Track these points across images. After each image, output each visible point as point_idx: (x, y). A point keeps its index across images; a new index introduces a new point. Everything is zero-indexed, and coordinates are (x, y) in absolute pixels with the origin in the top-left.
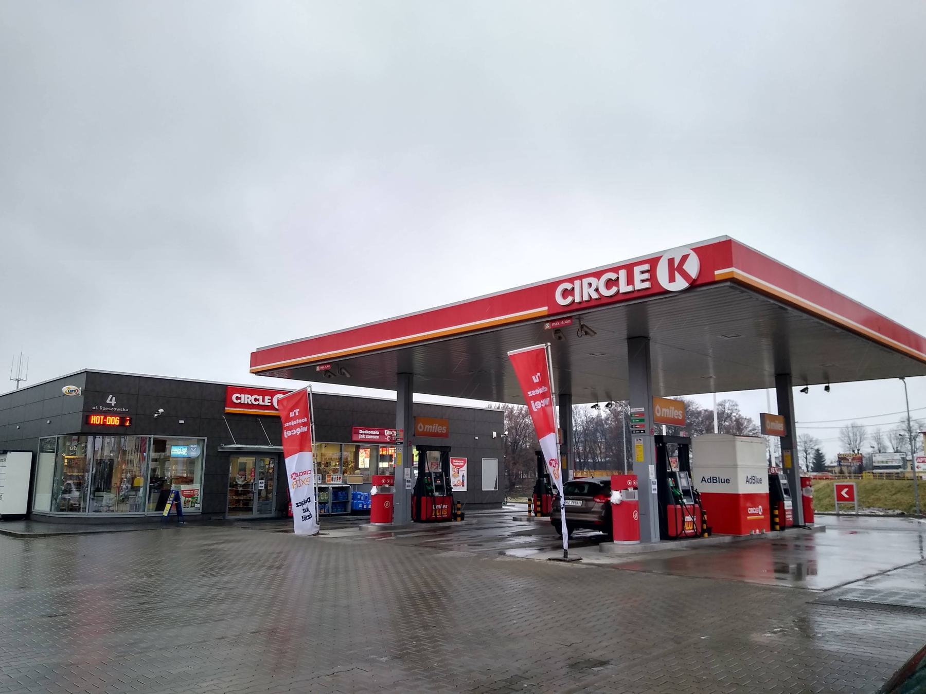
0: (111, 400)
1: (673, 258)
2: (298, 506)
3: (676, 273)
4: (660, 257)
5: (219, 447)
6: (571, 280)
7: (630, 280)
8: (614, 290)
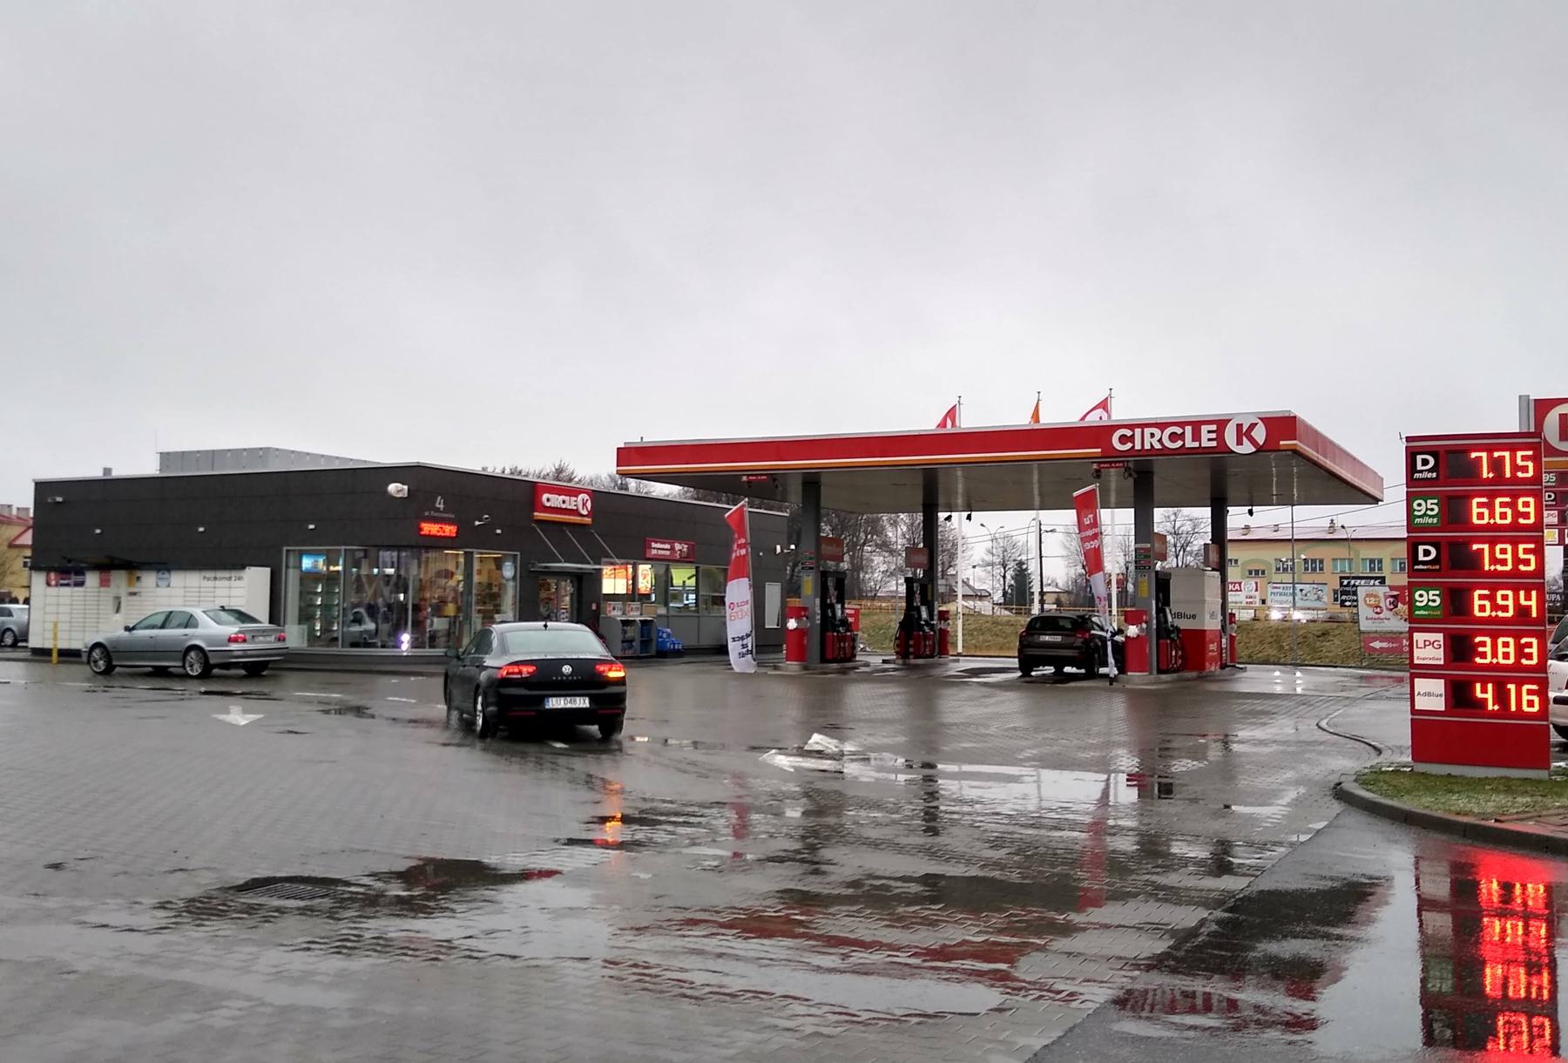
0: (440, 504)
1: (1242, 425)
2: (735, 641)
3: (1244, 438)
4: (1230, 420)
5: (530, 566)
6: (1131, 427)
7: (1196, 436)
8: (1179, 443)
